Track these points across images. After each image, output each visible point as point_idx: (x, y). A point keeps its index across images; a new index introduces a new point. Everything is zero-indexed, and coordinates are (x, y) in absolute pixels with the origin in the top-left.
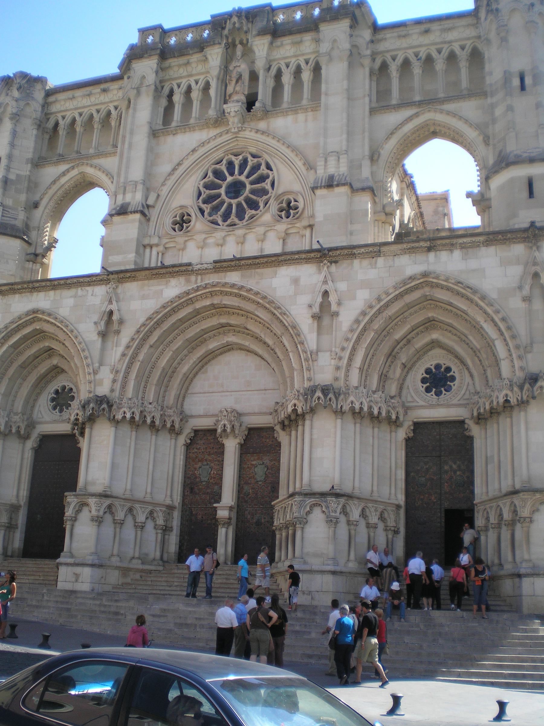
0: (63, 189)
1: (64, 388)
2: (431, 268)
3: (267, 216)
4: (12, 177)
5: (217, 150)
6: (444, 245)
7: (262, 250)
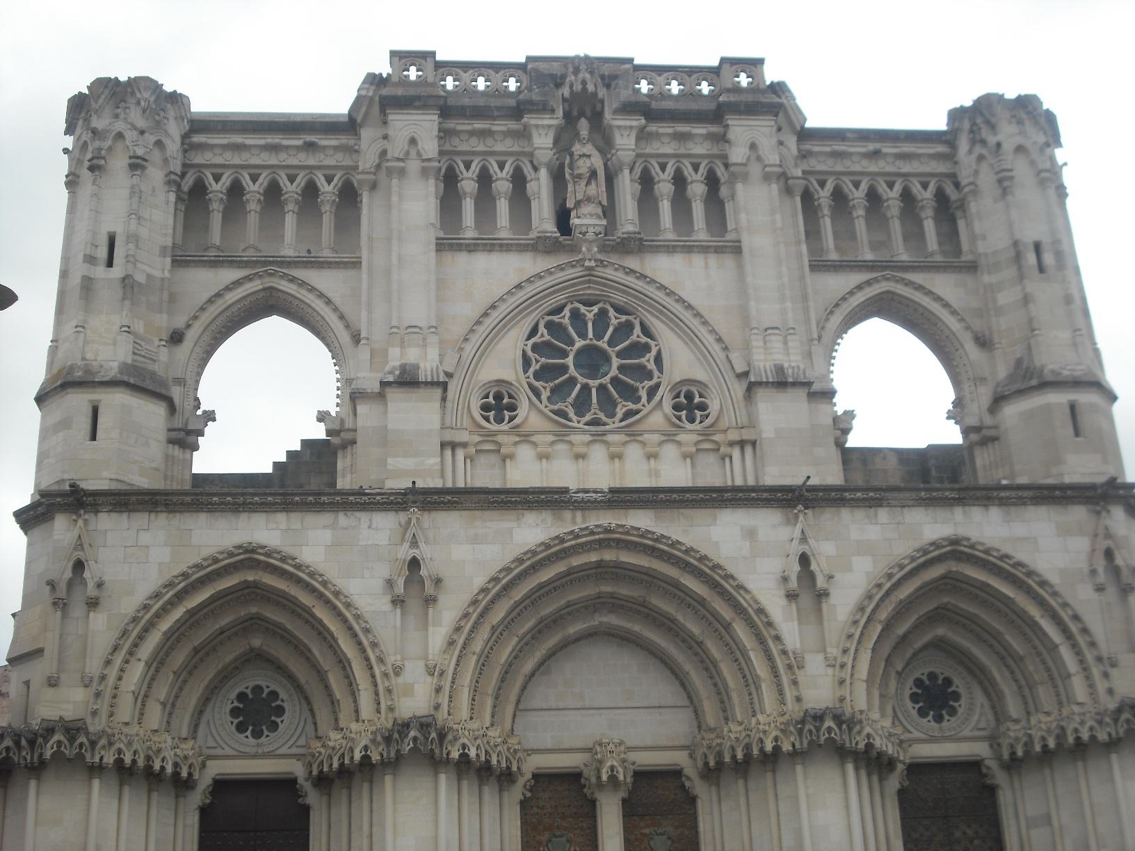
0: (228, 313)
1: (258, 689)
2: (962, 531)
3: (657, 417)
4: (140, 278)
5: (554, 292)
6: (977, 499)
7: (656, 473)
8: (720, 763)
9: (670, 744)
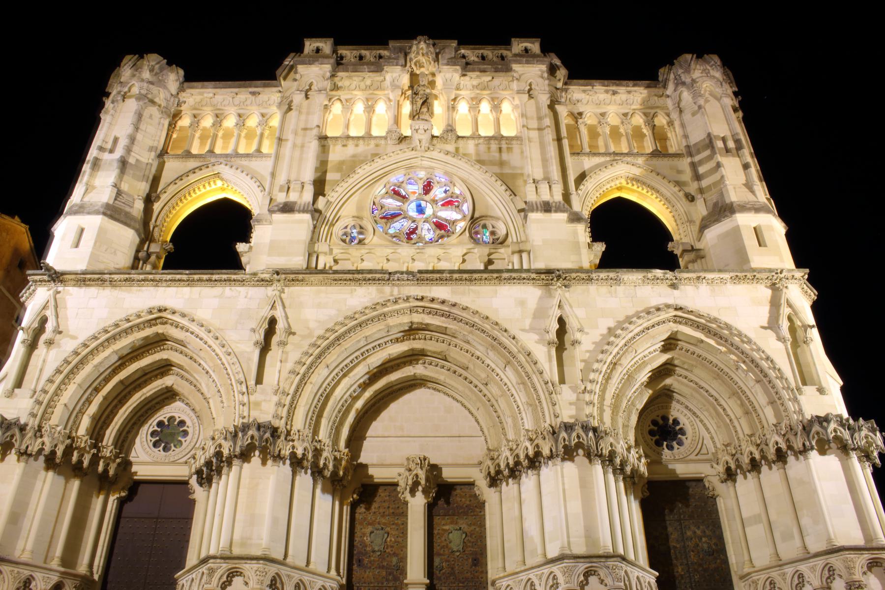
1: (171, 419)
4: (132, 160)
8: (498, 472)
9: (466, 462)
